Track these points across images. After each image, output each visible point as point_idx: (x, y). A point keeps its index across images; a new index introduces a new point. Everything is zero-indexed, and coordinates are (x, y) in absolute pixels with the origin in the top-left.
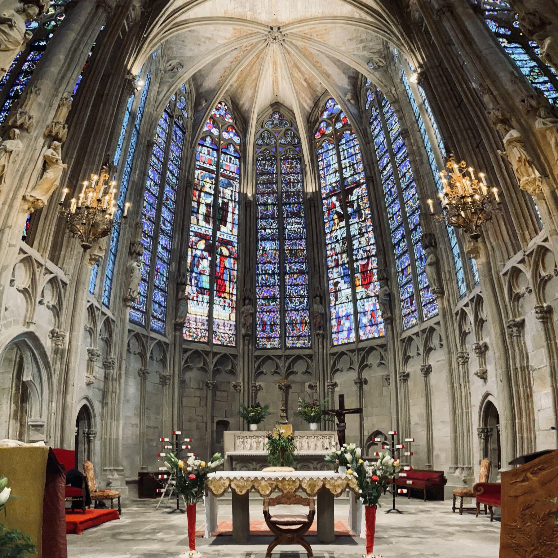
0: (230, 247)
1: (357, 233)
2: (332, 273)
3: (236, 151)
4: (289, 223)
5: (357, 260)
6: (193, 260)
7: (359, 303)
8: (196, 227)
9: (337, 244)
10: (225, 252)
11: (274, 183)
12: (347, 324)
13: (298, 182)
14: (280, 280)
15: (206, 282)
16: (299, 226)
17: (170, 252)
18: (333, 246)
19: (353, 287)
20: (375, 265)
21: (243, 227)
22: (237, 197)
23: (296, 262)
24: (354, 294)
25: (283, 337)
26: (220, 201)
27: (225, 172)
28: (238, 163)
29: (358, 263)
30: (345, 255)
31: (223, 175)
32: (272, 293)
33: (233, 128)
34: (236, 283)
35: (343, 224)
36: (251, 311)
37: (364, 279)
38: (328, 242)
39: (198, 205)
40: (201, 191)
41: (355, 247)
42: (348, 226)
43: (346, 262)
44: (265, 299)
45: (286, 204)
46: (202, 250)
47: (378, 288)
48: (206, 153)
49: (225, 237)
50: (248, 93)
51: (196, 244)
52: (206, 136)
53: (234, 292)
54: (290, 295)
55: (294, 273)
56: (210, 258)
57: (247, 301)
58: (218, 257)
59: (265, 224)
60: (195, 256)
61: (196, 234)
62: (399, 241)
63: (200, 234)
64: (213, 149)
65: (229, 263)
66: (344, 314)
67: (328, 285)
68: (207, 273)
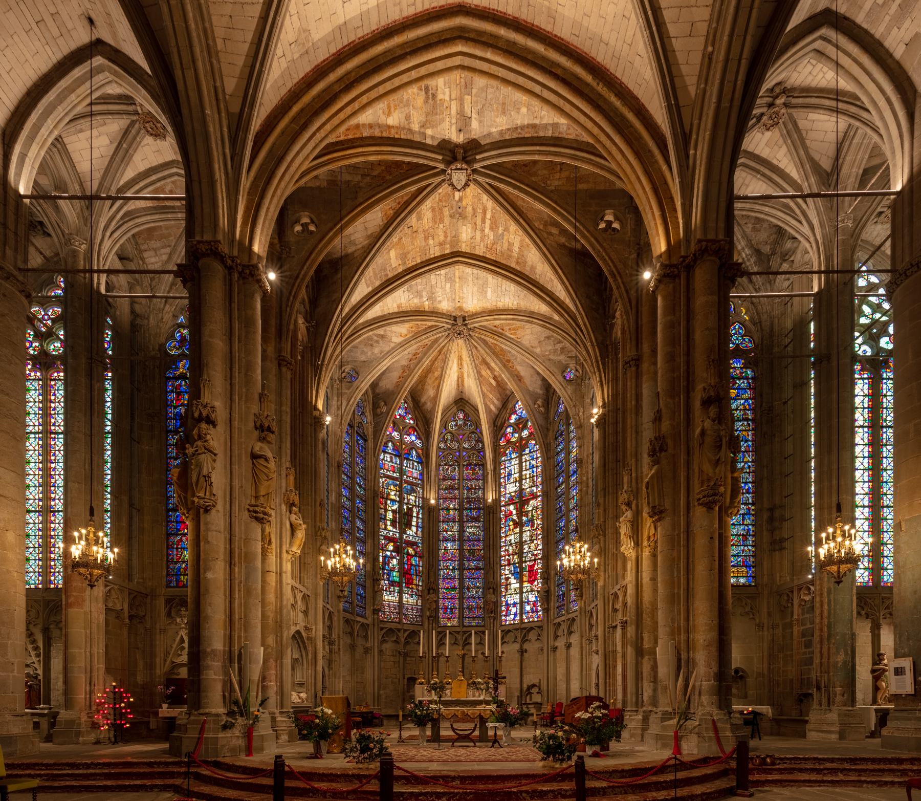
13: (480, 488)
21: (426, 530)
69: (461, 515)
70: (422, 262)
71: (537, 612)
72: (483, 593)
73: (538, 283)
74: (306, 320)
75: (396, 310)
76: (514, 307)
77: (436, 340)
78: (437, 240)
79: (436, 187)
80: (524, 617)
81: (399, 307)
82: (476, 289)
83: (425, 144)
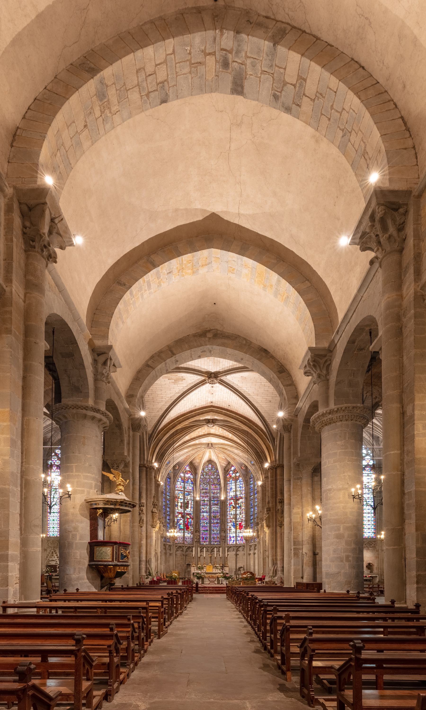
3: (191, 481)
6: (177, 521)
12: (233, 539)
15: (182, 527)
19: (236, 529)
24: (236, 531)
25: (210, 541)
26: (186, 501)
31: (186, 491)
33: (190, 472)
37: (240, 527)
40: (178, 498)
42: (236, 511)
61: (178, 513)
69: (210, 503)
71: (243, 540)
72: (220, 532)
80: (237, 542)
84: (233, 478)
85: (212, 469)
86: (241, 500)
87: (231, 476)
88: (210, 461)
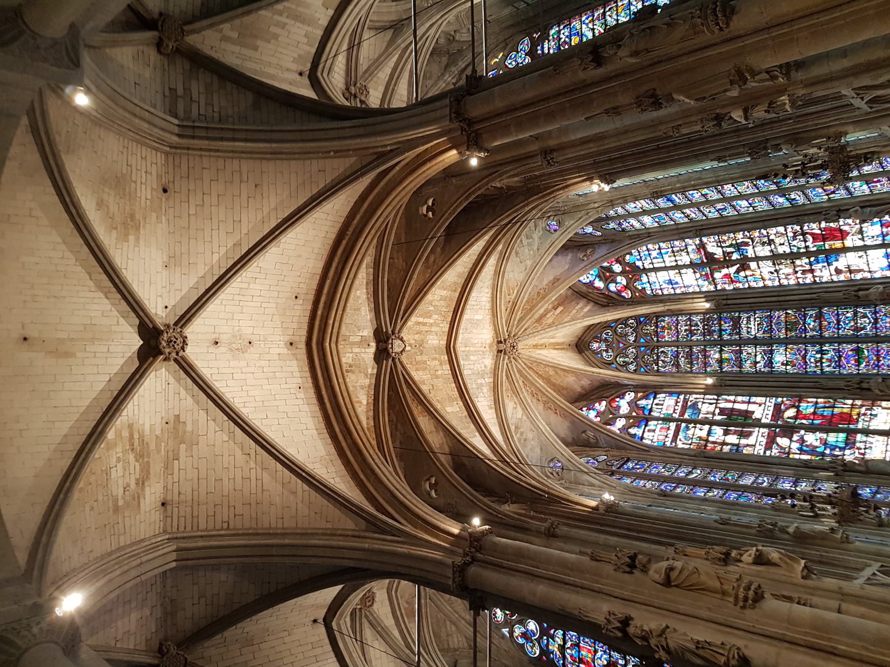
0: (783, 407)
1: (767, 248)
2: (822, 277)
3: (646, 397)
4: (748, 333)
5: (807, 247)
6: (806, 453)
7: (869, 242)
8: (758, 447)
9: (781, 272)
10: (791, 412)
11: (691, 350)
14: (831, 343)
15: (836, 438)
16: (752, 319)
17: (799, 479)
18: (783, 276)
19: (845, 250)
20: (814, 226)
22: (712, 397)
23: (804, 323)
24: (855, 249)
26: (718, 418)
27: (678, 412)
28: (664, 395)
29: (811, 246)
30: (798, 262)
31: (682, 413)
32: (850, 353)
33: (613, 400)
34: (835, 400)
35: (753, 265)
36: (880, 380)
37: (834, 238)
38: (776, 283)
39: (727, 444)
40: (707, 441)
41: (788, 251)
42: (757, 259)
43: (807, 260)
44: (858, 363)
45: (720, 336)
46: (791, 441)
47: (850, 221)
48: (652, 434)
49: (770, 413)
50: (571, 380)
51: (781, 448)
52: (629, 434)
53: (850, 402)
54: (853, 330)
55: (820, 325)
56: (802, 432)
57: (865, 385)
58: (798, 421)
59: (749, 362)
60: (800, 449)
61: (768, 447)
62: (787, 199)
63: (767, 443)
64: (646, 425)
65: (807, 408)
66: (885, 260)
67: (839, 282)
68: (824, 436)
70: (455, 382)
73: (471, 268)
74: (506, 503)
75: (494, 410)
76: (490, 291)
77: (519, 371)
78: (439, 367)
79: (403, 367)
81: (491, 408)
82: (474, 331)
83: (377, 374)
84: (629, 281)
85: (606, 340)
86: (712, 247)
87: (626, 287)
88: (580, 346)
